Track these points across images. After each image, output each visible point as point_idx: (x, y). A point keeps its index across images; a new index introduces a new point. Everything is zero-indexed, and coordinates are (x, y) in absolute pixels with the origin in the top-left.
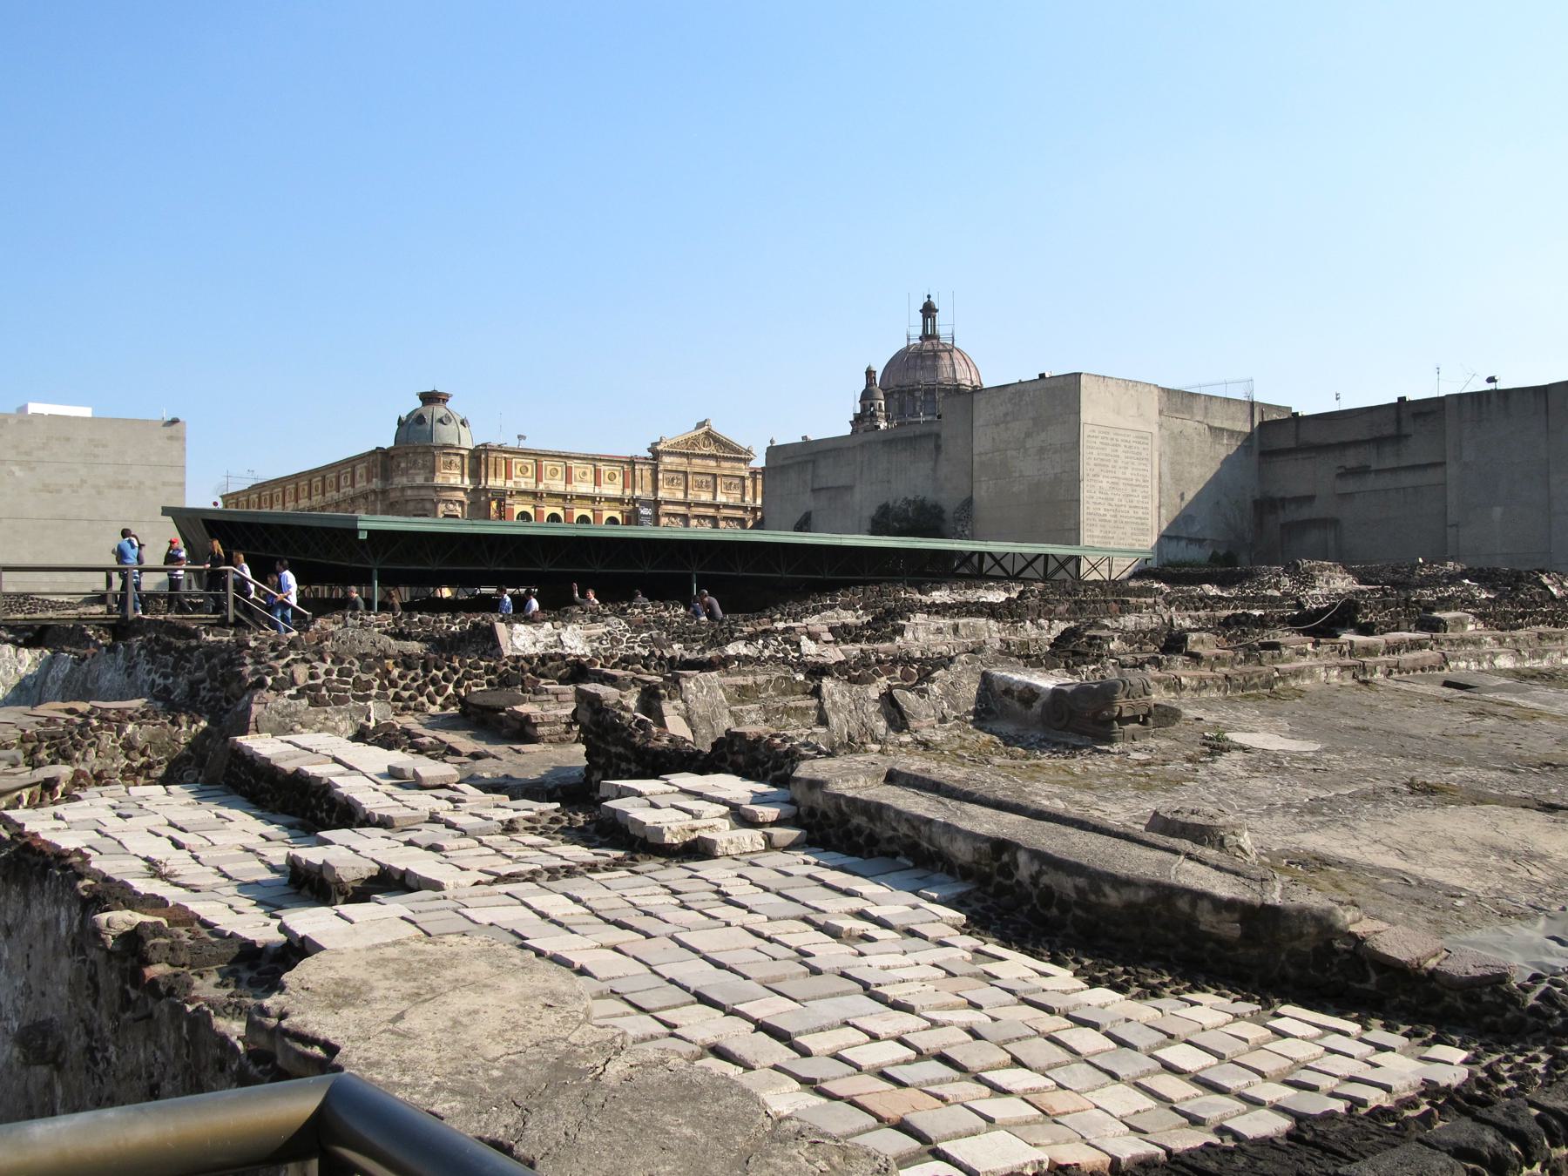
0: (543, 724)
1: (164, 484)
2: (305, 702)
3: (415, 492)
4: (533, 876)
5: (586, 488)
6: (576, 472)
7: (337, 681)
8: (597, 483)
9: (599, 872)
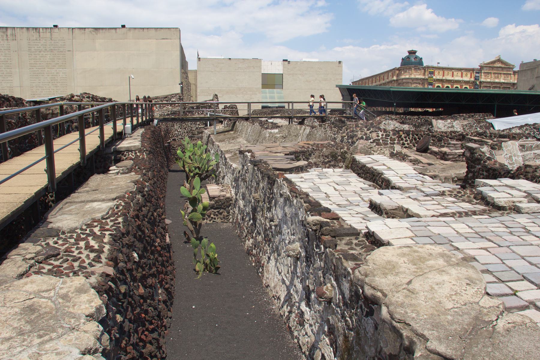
0: (451, 155)
1: (337, 79)
2: (375, 144)
3: (406, 80)
4: (453, 215)
6: (455, 73)
8: (462, 77)
9: (477, 215)
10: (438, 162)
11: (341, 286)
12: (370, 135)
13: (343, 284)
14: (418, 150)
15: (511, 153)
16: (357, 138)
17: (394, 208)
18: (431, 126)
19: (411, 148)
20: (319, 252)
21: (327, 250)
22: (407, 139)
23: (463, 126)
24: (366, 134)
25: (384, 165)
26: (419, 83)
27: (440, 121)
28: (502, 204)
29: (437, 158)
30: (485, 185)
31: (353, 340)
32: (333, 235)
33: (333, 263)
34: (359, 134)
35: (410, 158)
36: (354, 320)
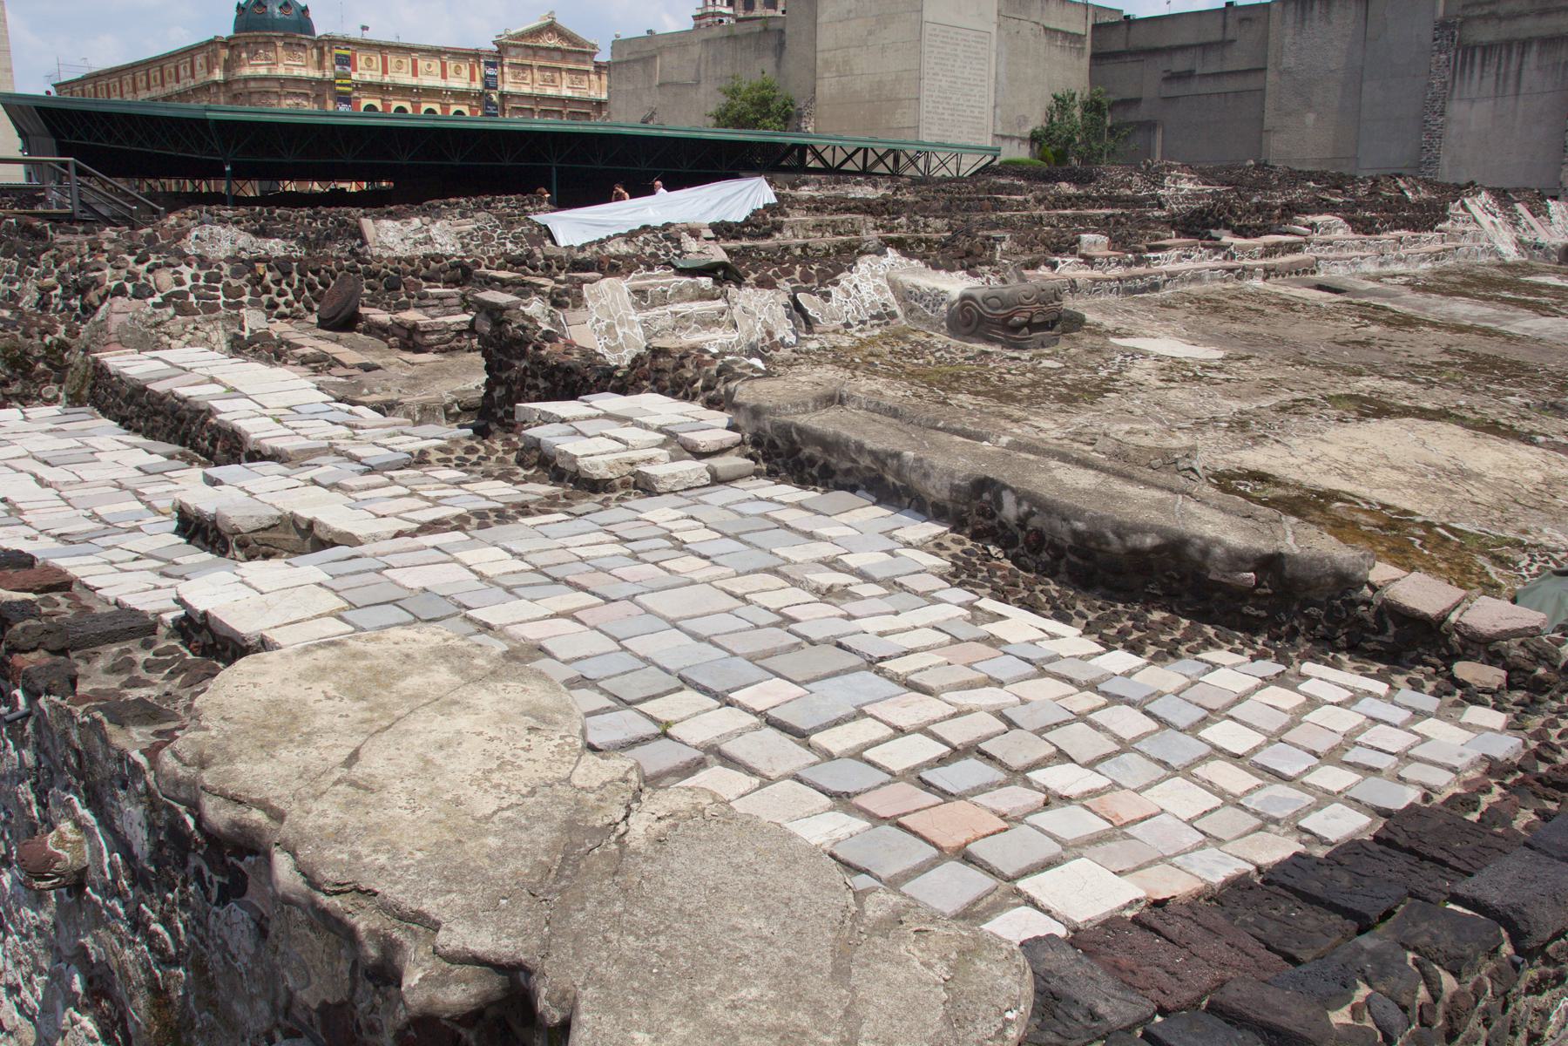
0: (433, 332)
2: (171, 311)
4: (460, 523)
5: (433, 81)
6: (422, 64)
7: (205, 287)
8: (444, 76)
9: (533, 515)
10: (393, 359)
11: (112, 819)
12: (151, 277)
13: (120, 811)
14: (323, 324)
15: (610, 316)
16: (102, 291)
17: (267, 523)
18: (359, 241)
19: (301, 319)
20: (7, 718)
21: (42, 701)
22: (284, 286)
23: (462, 237)
24: (133, 276)
25: (213, 380)
26: (306, 96)
27: (387, 224)
28: (601, 472)
29: (391, 347)
30: (547, 419)
31: (186, 995)
32: (57, 644)
33: (69, 744)
34: (109, 279)
35: (299, 352)
36: (180, 925)
